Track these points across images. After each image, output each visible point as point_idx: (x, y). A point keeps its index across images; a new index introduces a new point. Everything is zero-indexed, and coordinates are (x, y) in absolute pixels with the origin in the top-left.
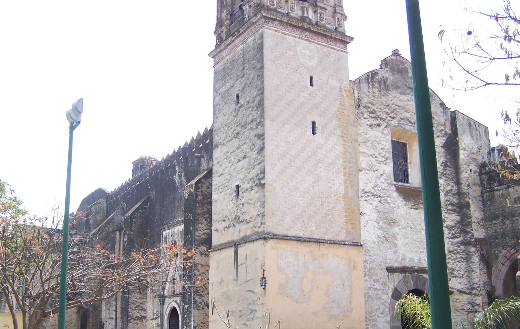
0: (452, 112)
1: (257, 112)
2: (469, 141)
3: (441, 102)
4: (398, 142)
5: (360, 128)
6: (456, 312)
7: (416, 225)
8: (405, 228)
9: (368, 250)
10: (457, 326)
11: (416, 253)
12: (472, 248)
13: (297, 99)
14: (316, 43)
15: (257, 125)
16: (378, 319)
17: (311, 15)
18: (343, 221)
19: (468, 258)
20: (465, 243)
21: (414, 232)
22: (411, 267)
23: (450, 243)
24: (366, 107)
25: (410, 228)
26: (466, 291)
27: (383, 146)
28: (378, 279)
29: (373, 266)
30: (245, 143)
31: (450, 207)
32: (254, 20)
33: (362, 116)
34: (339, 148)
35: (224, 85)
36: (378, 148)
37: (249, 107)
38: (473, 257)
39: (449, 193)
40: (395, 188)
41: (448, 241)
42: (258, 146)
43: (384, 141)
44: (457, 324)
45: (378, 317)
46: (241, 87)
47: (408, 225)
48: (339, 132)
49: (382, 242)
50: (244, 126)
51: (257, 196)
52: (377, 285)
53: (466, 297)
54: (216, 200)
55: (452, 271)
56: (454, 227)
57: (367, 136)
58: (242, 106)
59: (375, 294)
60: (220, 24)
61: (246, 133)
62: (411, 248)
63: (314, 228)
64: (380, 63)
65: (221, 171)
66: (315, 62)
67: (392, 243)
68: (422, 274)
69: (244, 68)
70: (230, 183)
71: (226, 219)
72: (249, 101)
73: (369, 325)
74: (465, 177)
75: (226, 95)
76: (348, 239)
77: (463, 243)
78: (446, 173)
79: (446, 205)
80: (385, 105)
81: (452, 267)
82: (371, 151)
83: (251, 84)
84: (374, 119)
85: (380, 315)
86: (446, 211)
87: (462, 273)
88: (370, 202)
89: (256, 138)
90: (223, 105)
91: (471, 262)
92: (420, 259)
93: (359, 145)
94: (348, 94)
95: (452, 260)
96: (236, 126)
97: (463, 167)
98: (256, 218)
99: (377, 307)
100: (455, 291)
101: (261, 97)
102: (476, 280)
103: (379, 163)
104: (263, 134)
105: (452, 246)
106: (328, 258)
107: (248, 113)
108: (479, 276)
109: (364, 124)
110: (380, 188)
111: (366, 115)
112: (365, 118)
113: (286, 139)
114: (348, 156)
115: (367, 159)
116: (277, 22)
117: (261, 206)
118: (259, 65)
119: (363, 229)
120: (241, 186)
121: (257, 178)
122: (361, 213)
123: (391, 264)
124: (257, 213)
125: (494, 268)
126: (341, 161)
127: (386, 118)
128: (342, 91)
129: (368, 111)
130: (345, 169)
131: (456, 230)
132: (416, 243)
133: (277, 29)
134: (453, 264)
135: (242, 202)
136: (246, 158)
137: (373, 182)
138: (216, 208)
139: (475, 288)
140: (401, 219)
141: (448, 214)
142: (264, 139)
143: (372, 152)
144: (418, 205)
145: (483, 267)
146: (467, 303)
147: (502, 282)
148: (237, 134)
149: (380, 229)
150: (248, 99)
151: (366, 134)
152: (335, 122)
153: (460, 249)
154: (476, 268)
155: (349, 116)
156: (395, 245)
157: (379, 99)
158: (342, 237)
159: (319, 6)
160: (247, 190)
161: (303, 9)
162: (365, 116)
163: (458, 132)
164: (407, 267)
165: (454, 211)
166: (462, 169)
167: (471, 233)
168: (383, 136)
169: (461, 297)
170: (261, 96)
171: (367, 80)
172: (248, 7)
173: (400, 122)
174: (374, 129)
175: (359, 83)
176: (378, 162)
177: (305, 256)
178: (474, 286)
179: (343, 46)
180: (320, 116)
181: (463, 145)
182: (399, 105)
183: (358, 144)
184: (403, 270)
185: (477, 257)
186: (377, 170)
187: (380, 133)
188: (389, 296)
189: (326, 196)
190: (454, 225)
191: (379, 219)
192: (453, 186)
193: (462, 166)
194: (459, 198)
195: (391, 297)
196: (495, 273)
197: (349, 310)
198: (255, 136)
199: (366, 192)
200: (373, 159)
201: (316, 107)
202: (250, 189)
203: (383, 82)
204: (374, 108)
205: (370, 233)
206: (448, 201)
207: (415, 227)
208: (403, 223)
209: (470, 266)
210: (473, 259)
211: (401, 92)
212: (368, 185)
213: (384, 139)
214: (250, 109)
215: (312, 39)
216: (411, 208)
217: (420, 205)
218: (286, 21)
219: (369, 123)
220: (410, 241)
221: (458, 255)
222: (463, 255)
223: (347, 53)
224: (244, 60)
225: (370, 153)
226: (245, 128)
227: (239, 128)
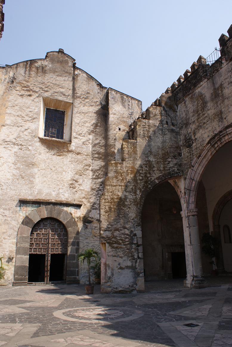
2: (120, 109)
3: (98, 83)
4: (56, 110)
5: (10, 96)
6: (94, 237)
7: (57, 167)
8: (44, 169)
16: (4, 240)
21: (54, 173)
24: (19, 83)
25: (49, 170)
27: (31, 110)
28: (9, 208)
29: (4, 197)
31: (97, 156)
39: (96, 145)
40: (39, 140)
43: (33, 106)
44: (94, 247)
45: (4, 238)
47: (48, 167)
49: (18, 179)
52: (7, 213)
56: (98, 170)
57: (16, 103)
59: (3, 221)
74: (112, 134)
78: (96, 131)
79: (93, 154)
80: (40, 83)
82: (18, 113)
84: (26, 91)
85: (6, 237)
88: (10, 148)
92: (58, 194)
93: (7, 108)
99: (5, 231)
100: (95, 221)
105: (95, 185)
112: (17, 90)
115: (13, 118)
123: (26, 197)
127: (40, 91)
131: (100, 172)
132: (55, 181)
140: (42, 163)
141: (94, 160)
143: (20, 113)
144: (61, 152)
149: (16, 169)
151: (16, 101)
156: (32, 182)
162: (17, 89)
163: (110, 102)
164: (43, 200)
165: (100, 158)
168: (33, 102)
176: (24, 120)
181: (113, 111)
183: (6, 107)
184: (37, 203)
188: (18, 222)
190: (99, 169)
191: (16, 162)
192: (101, 140)
193: (111, 126)
199: (6, 142)
200: (19, 120)
203: (41, 68)
204: (29, 84)
205: (5, 172)
206: (95, 151)
207: (56, 169)
208: (42, 166)
211: (58, 75)
212: (10, 136)
216: (54, 155)
217: (64, 153)
219: (20, 94)
220: (49, 180)
221: (99, 192)
225: (17, 114)
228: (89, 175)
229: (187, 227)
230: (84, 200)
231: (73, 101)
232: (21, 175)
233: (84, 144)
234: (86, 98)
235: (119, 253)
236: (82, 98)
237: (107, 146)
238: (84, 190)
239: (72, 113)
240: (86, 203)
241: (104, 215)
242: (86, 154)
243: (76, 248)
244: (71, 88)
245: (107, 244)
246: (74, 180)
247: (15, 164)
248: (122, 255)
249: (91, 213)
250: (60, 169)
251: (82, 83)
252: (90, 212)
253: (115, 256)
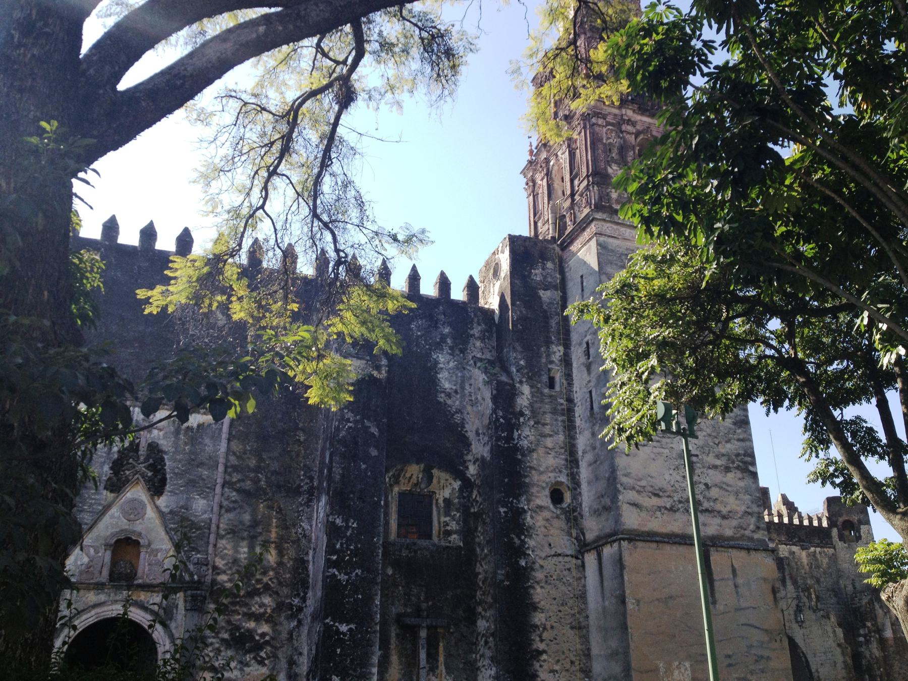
71: (661, 494)
124: (743, 508)
160: (715, 467)
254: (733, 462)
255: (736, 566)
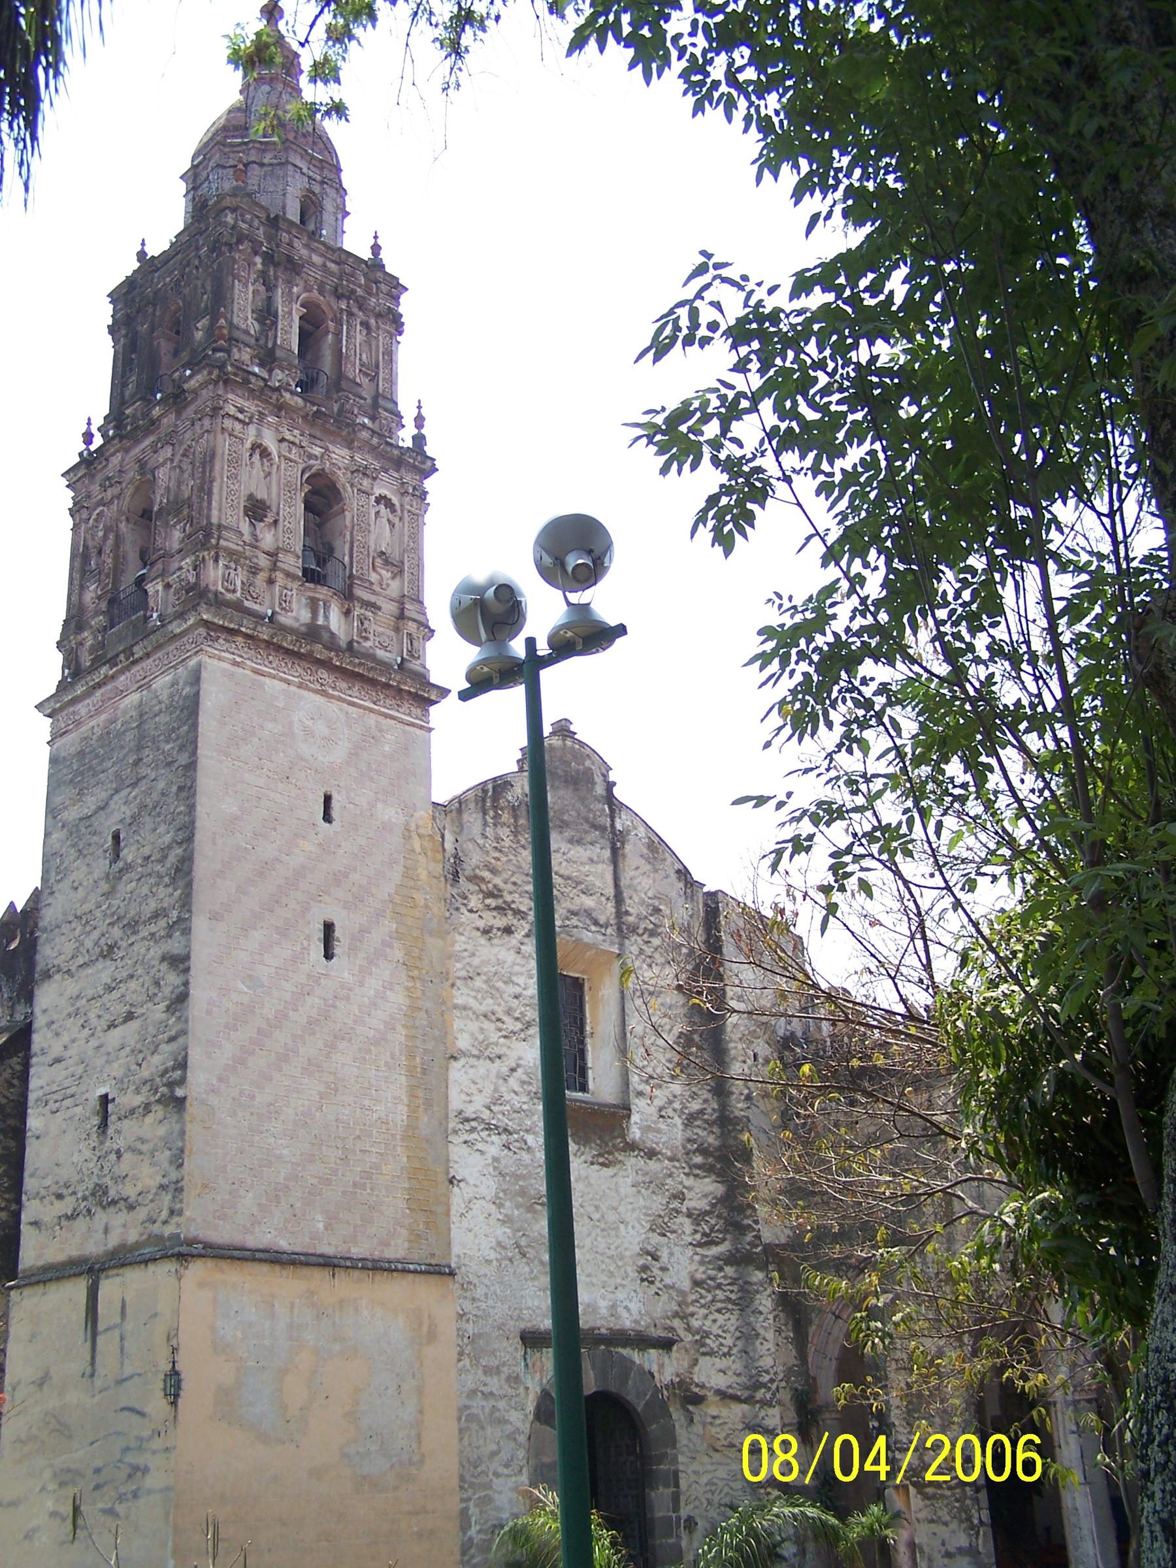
0: (709, 894)
1: (170, 890)
3: (681, 867)
5: (458, 937)
6: (712, 1453)
9: (470, 1283)
10: (713, 1493)
11: (603, 1291)
12: (757, 1272)
13: (285, 858)
14: (344, 701)
15: (171, 927)
16: (495, 1480)
17: (335, 621)
18: (402, 1205)
19: (744, 1302)
20: (735, 1259)
22: (589, 1329)
23: (697, 1258)
24: (475, 879)
25: (586, 1220)
26: (739, 1393)
27: (518, 990)
28: (498, 1367)
30: (132, 976)
31: (698, 1159)
32: (176, 628)
33: (465, 905)
34: (397, 999)
35: (80, 800)
36: (505, 996)
37: (150, 875)
38: (758, 1296)
39: (695, 1119)
41: (691, 1253)
42: (170, 989)
43: (521, 974)
44: (713, 1488)
45: (497, 1475)
46: (128, 814)
48: (398, 954)
49: (511, 1260)
50: (132, 926)
51: (162, 1131)
52: (494, 1384)
53: (739, 1409)
54: (38, 1133)
55: (702, 1337)
56: (707, 1213)
57: (476, 961)
58: (128, 868)
59: (487, 1410)
60: (75, 621)
61: (136, 948)
62: (589, 1275)
63: (321, 1226)
64: (519, 756)
65: (56, 1050)
66: (339, 754)
67: (536, 1262)
68: (620, 1350)
69: (140, 760)
70: (83, 1088)
71: (65, 1192)
72: (149, 857)
73: (469, 1499)
75: (83, 830)
76: (415, 1256)
77: (730, 1259)
79: (687, 1154)
81: (701, 1327)
83: (158, 809)
84: (495, 913)
85: (501, 1470)
86: (687, 1170)
87: (729, 1341)
88: (479, 1146)
89: (164, 967)
90: (72, 858)
91: (753, 1312)
92: (613, 1307)
93: (453, 985)
94: (428, 844)
95: (703, 1306)
96: (109, 924)
97: (735, 1047)
98: (156, 1194)
99: (494, 1447)
101: (185, 850)
102: (767, 1362)
103: (505, 1037)
104: (187, 957)
105: (702, 1269)
106: (356, 1309)
107: (145, 890)
108: (773, 1350)
109: (469, 928)
110: (508, 1107)
111: (474, 902)
112: (471, 911)
113: (250, 972)
114: (421, 1019)
115: (473, 1026)
116: (240, 639)
117: (171, 1162)
118: (183, 759)
119: (458, 1225)
120: (114, 1099)
121: (165, 1080)
122: (454, 1177)
124: (159, 1180)
125: (814, 1327)
126: (400, 1035)
128: (410, 837)
129: (481, 891)
130: (411, 1056)
131: (713, 1222)
132: (603, 1262)
133: (239, 659)
134: (706, 1317)
135: (115, 1147)
136: (132, 1019)
137: (489, 1089)
138: (36, 1155)
139: (764, 1385)
141: (692, 1177)
142: (187, 970)
143: (488, 1005)
144: (610, 1153)
145: (785, 1325)
146: (740, 1426)
147: (834, 1362)
148: (111, 948)
149: (504, 1222)
150: (146, 851)
152: (388, 925)
153: (725, 1277)
154: (766, 1329)
155: (427, 907)
157: (512, 857)
158: (397, 1250)
159: (359, 599)
160: (132, 1112)
161: (313, 604)
162: (472, 905)
165: (709, 1169)
166: (733, 1052)
167: (754, 1230)
168: (519, 960)
169: (724, 1412)
170: (184, 846)
171: (480, 805)
172: (160, 587)
173: (568, 922)
174: (495, 941)
175: (460, 811)
176: (504, 1033)
177: (292, 1306)
178: (761, 1379)
179: (419, 711)
180: (347, 906)
182: (566, 873)
183: (450, 982)
185: (770, 1296)
186: (499, 1057)
187: (512, 952)
188: (526, 1415)
189: (358, 1133)
190: (708, 1208)
191: (501, 1195)
192: (706, 1101)
193: (732, 1045)
194: (722, 1133)
195: (531, 1417)
196: (815, 1340)
197: (415, 1459)
198: (163, 959)
199: (467, 1120)
200: (489, 1026)
201: (337, 882)
202: (141, 1110)
204: (498, 881)
205: (476, 1236)
207: (603, 1216)
209: (749, 1324)
210: (757, 1302)
212: (474, 1098)
213: (523, 970)
214: (152, 881)
215: (334, 688)
216: (592, 1163)
217: (616, 1154)
218: (265, 637)
219: (481, 924)
220: (588, 1256)
221: (718, 1292)
222: (732, 1292)
223: (430, 730)
224: (142, 737)
225: (483, 1008)
226: (135, 933)
227: (116, 932)
228: (684, 1232)
229: (1073, 1432)
230: (676, 1323)
231: (621, 945)
232: (518, 1246)
233: (662, 1116)
234: (653, 933)
235: (940, 1513)
236: (640, 931)
237: (725, 1122)
238: (672, 1287)
239: (618, 995)
240: (682, 1333)
241: (898, 1407)
242: (669, 1153)
243: (673, 1493)
244: (610, 891)
245: (911, 1489)
246: (648, 1253)
247: (498, 1203)
248: (947, 1518)
249: (696, 1369)
250: (612, 1217)
251: (637, 868)
252: (695, 1364)
253: (932, 1521)
254: (156, 1091)
255: (127, 1299)
